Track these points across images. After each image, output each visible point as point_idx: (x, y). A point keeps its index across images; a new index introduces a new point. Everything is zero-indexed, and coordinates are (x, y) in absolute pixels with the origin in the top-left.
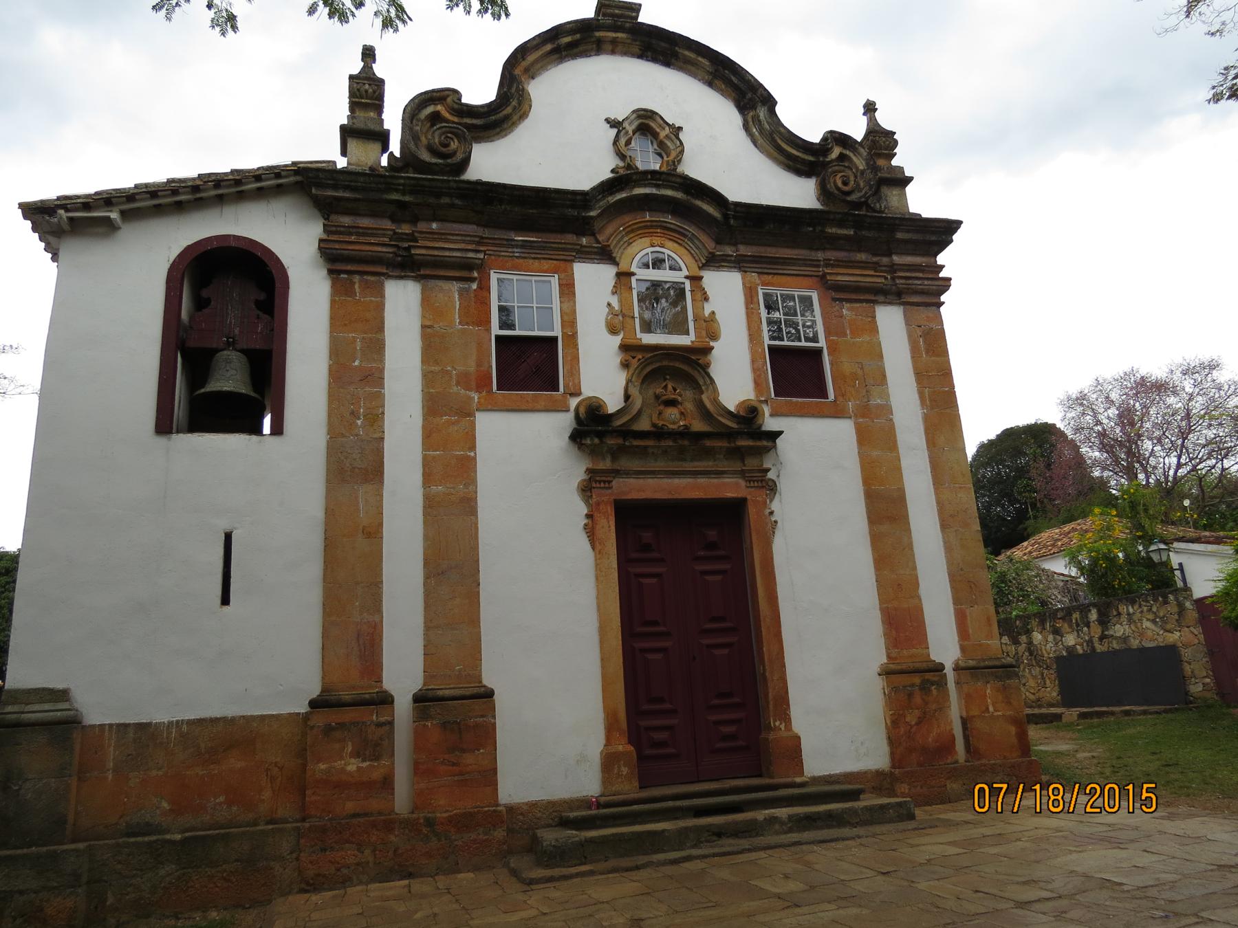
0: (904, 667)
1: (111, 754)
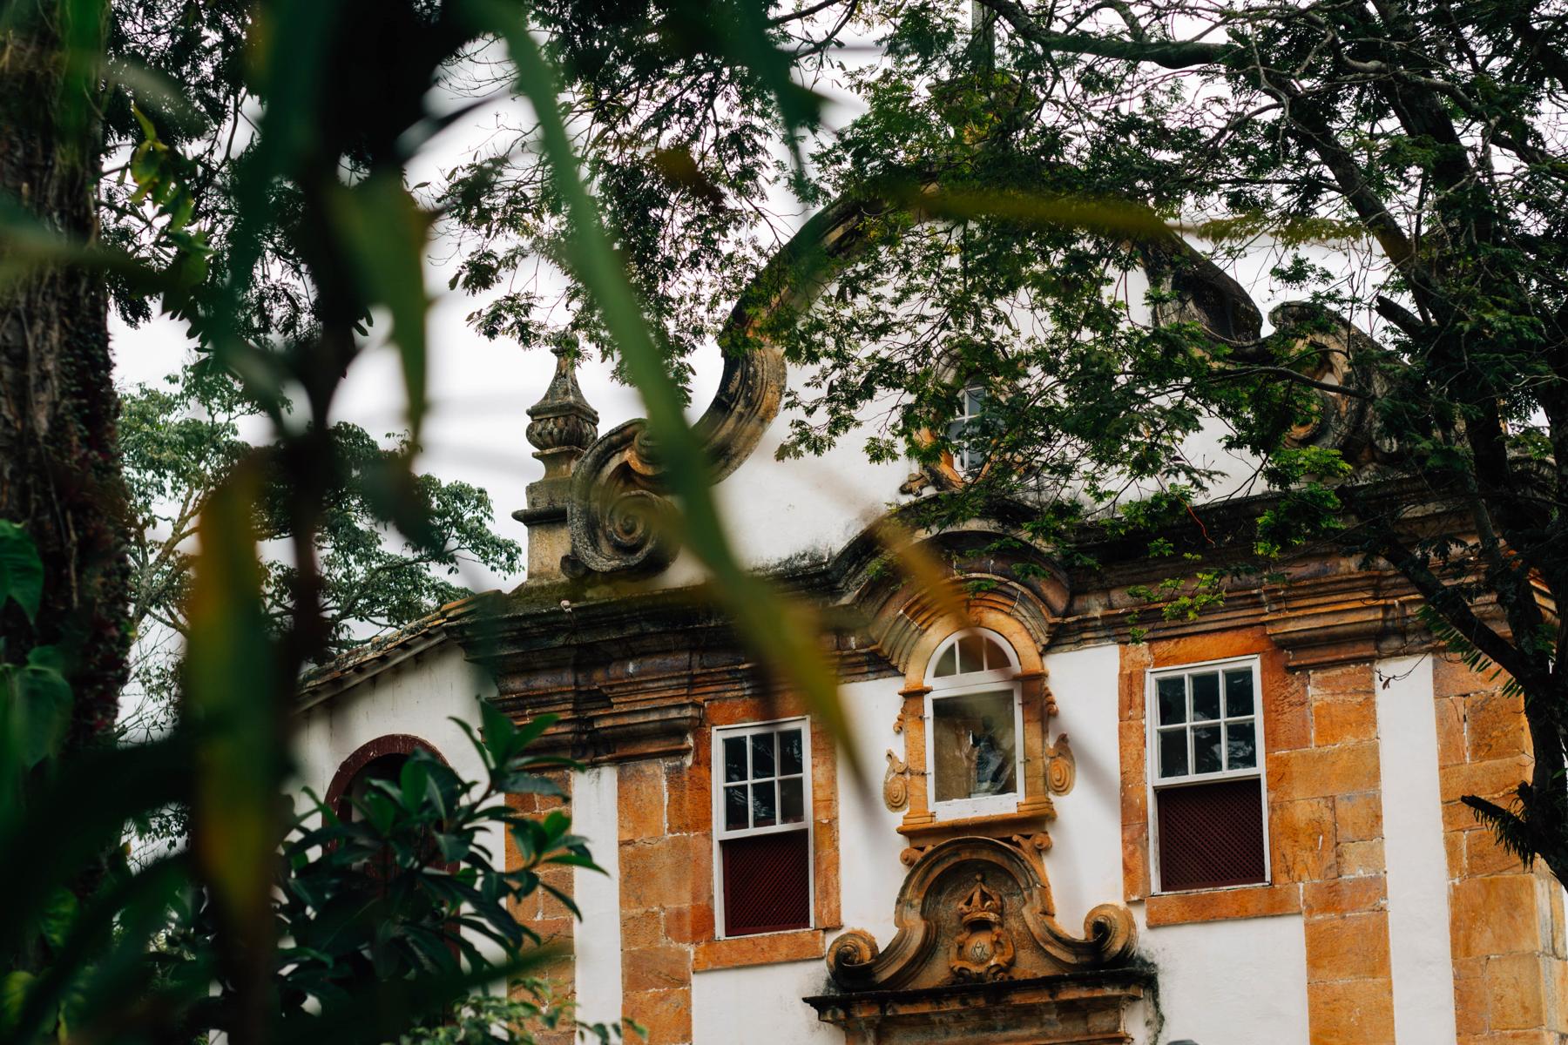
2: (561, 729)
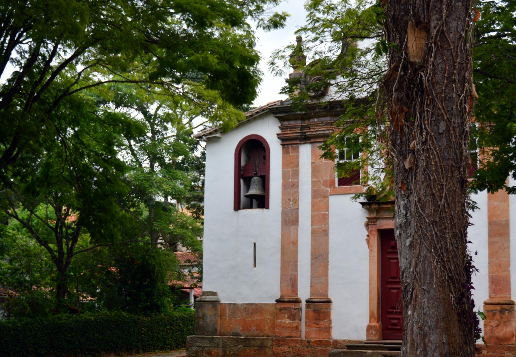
0: (493, 302)
1: (228, 312)
2: (297, 134)
